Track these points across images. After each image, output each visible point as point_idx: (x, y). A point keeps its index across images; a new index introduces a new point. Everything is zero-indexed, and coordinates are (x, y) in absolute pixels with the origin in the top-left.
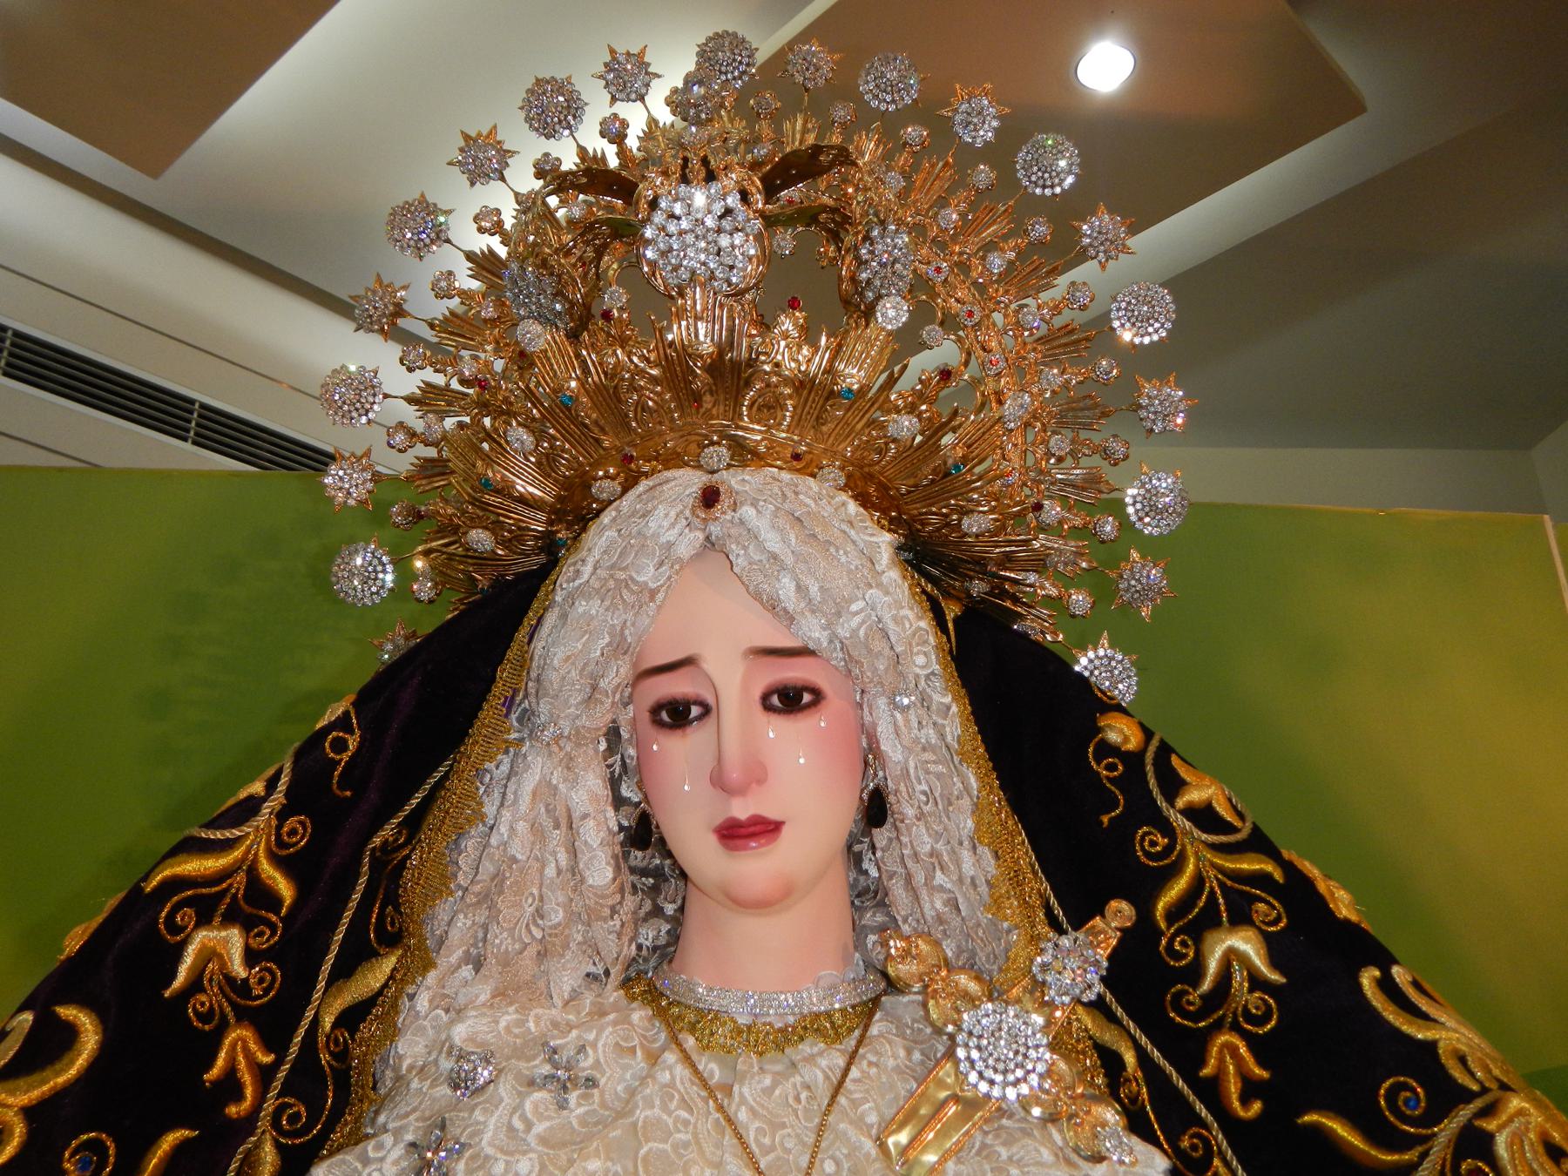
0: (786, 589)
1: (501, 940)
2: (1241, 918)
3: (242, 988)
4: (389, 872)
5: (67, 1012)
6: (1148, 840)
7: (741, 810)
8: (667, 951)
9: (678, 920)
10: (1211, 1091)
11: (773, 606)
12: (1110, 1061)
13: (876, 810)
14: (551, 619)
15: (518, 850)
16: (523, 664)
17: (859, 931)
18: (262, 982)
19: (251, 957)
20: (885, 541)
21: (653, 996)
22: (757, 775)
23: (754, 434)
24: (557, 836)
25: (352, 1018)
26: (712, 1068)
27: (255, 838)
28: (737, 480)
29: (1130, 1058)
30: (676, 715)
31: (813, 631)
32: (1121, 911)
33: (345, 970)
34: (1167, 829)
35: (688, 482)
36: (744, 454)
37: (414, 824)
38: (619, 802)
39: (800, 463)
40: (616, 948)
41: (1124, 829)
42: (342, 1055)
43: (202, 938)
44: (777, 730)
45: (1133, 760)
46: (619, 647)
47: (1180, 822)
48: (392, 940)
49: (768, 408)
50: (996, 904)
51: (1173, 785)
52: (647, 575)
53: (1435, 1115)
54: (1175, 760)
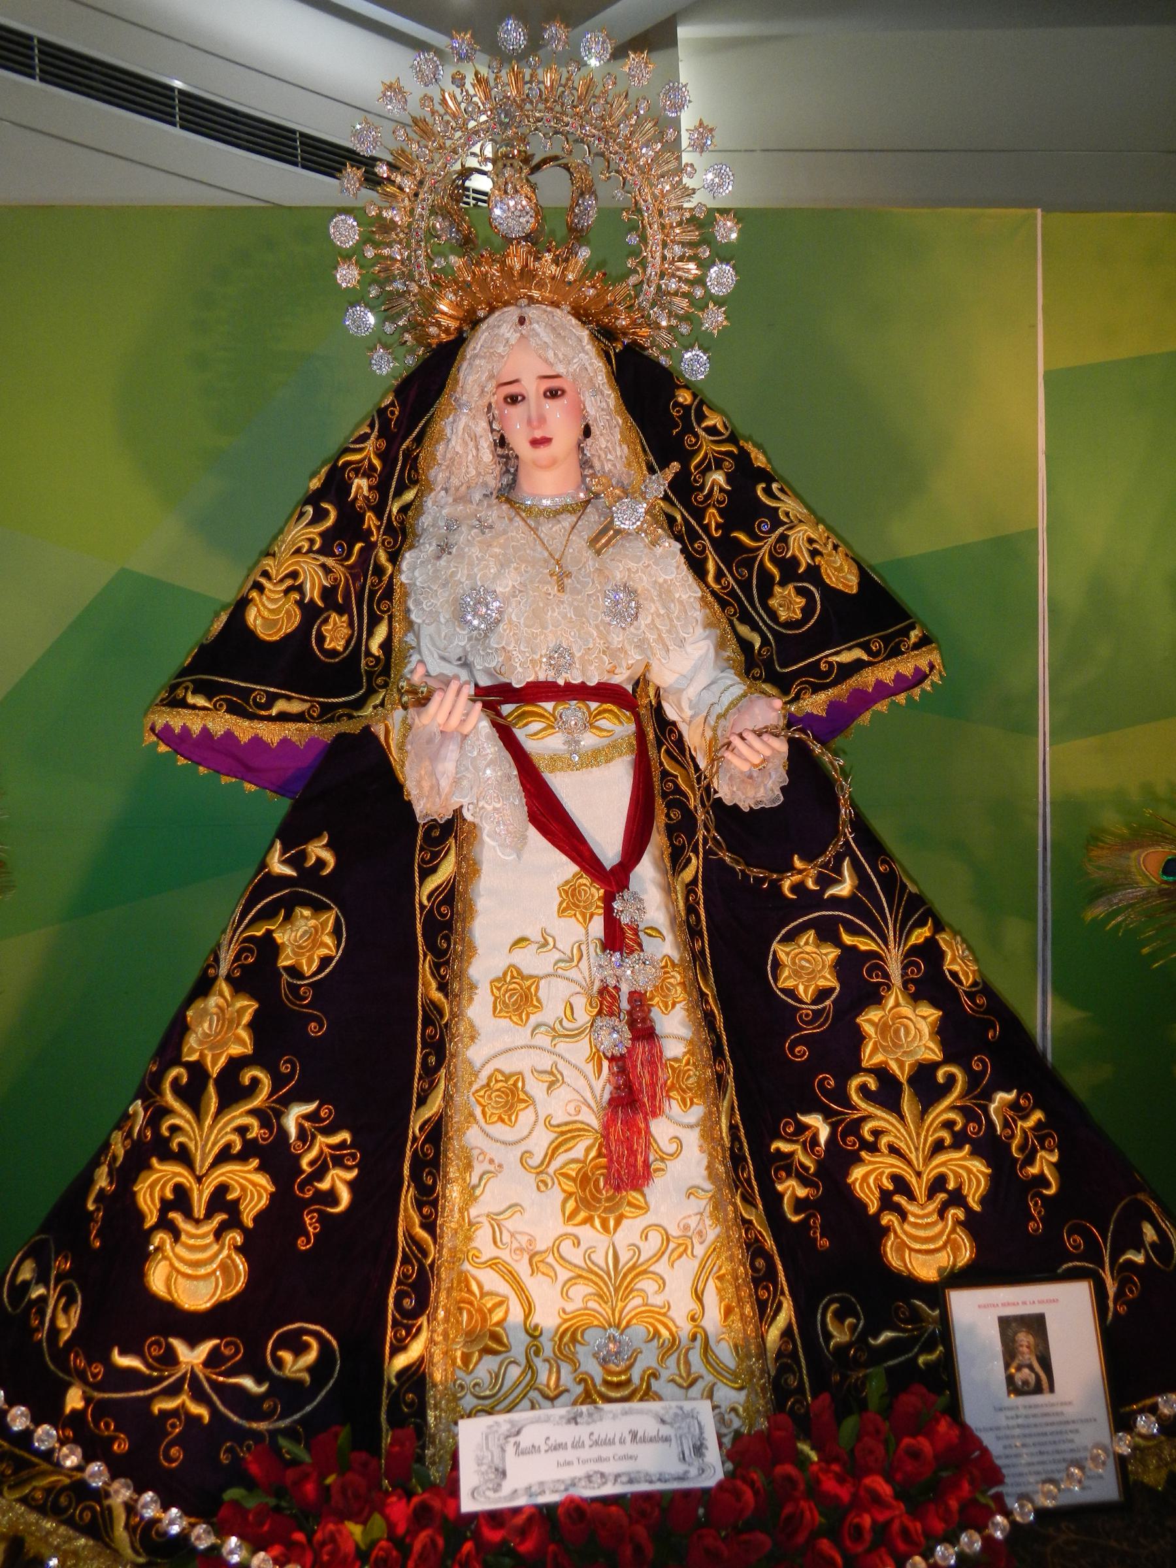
0: (550, 355)
1: (455, 481)
2: (719, 467)
3: (366, 498)
4: (412, 461)
5: (325, 505)
6: (689, 439)
7: (538, 434)
8: (513, 485)
9: (515, 474)
10: (706, 529)
11: (546, 361)
12: (671, 520)
13: (587, 432)
14: (465, 365)
15: (459, 449)
16: (456, 381)
17: (584, 477)
18: (374, 497)
19: (370, 488)
20: (585, 334)
21: (508, 501)
22: (542, 420)
23: (536, 294)
24: (471, 444)
25: (404, 509)
26: (533, 524)
27: (370, 446)
28: (532, 312)
29: (679, 518)
30: (513, 400)
31: (561, 369)
32: (675, 466)
33: (399, 493)
34: (696, 436)
35: (512, 313)
36: (532, 300)
37: (419, 440)
38: (492, 430)
39: (556, 305)
40: (493, 483)
41: (681, 435)
42: (402, 523)
43: (356, 481)
44: (549, 405)
45: (687, 408)
46: (491, 377)
47: (702, 433)
48: (415, 482)
49: (541, 286)
50: (629, 465)
51: (701, 417)
52: (501, 349)
53: (772, 531)
54: (705, 408)
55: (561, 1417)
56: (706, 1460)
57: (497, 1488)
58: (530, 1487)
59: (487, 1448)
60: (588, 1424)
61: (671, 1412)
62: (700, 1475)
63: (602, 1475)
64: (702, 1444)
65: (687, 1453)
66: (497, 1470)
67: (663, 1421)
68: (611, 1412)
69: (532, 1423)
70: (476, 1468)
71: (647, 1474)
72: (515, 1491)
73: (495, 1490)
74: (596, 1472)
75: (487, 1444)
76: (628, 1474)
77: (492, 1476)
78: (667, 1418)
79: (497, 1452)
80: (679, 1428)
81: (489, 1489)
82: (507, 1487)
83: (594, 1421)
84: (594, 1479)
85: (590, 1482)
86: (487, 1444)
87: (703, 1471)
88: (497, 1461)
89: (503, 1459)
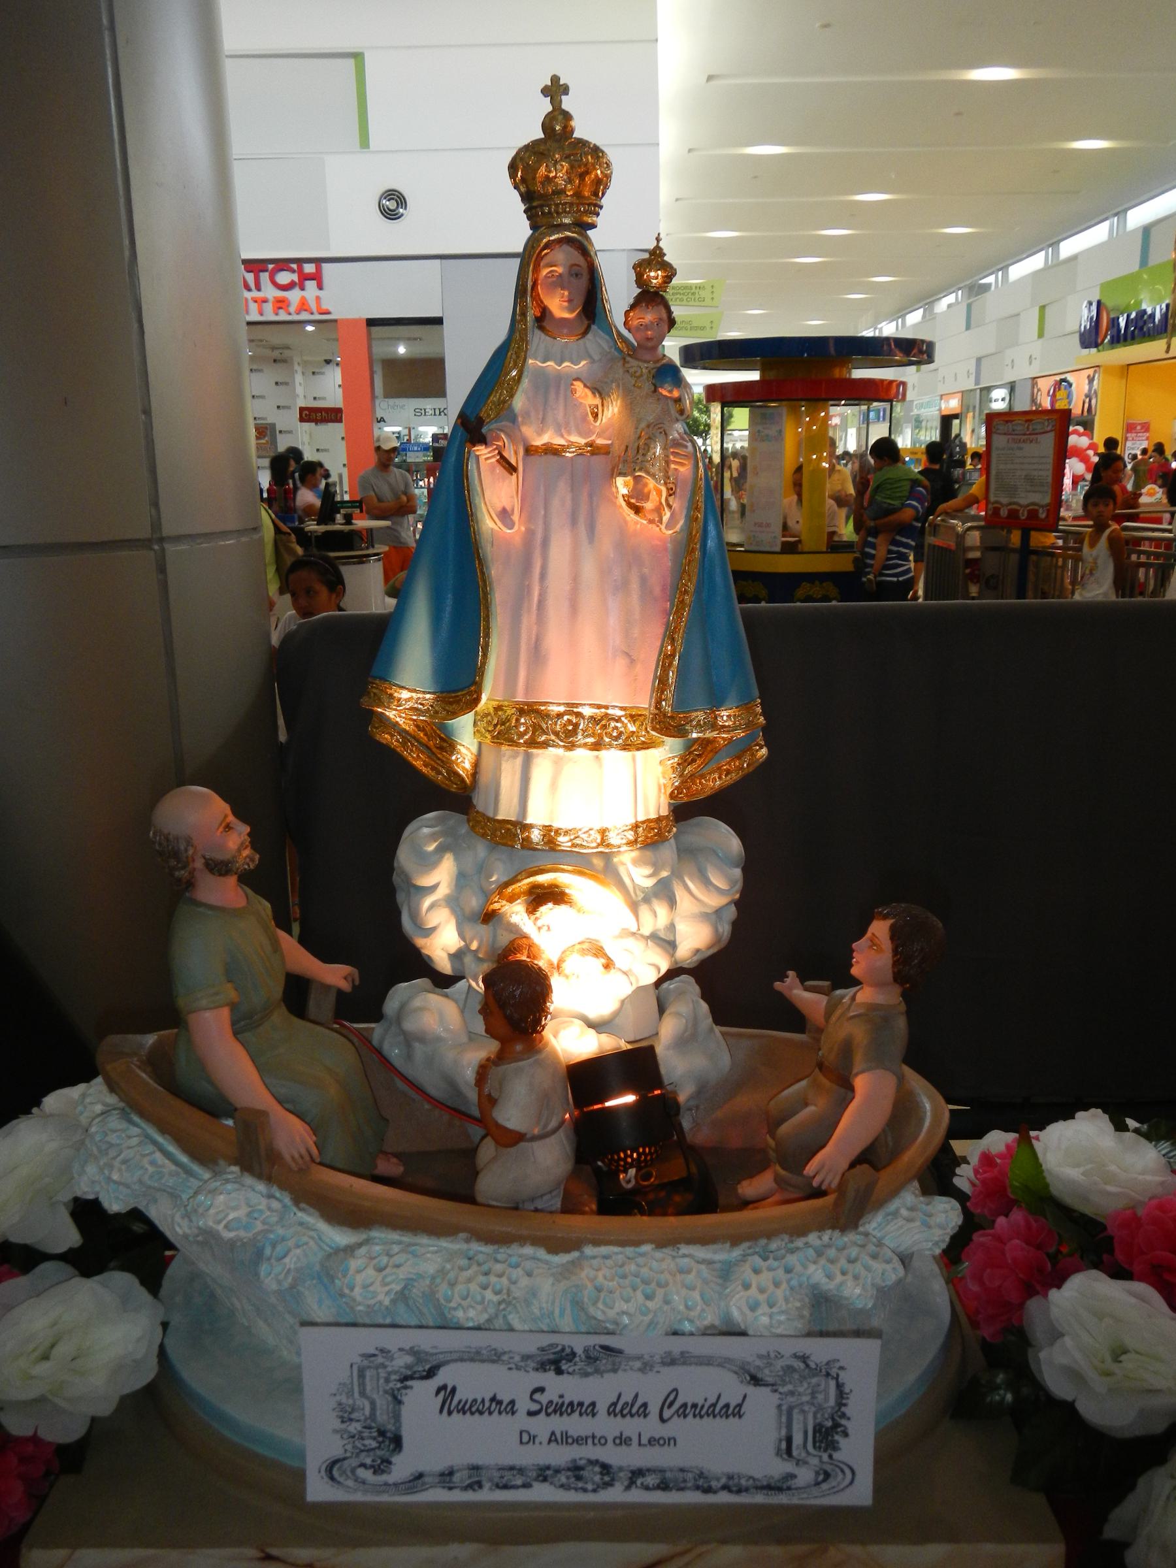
55: (526, 1357)
56: (836, 1455)
57: (382, 1466)
58: (451, 1473)
59: (363, 1393)
60: (586, 1375)
61: (780, 1364)
62: (817, 1484)
63: (605, 1468)
64: (836, 1425)
65: (798, 1439)
66: (382, 1433)
67: (756, 1381)
68: (639, 1358)
69: (462, 1360)
70: (337, 1424)
71: (701, 1475)
72: (420, 1476)
73: (377, 1471)
74: (592, 1463)
75: (362, 1385)
76: (662, 1471)
77: (374, 1444)
78: (767, 1375)
79: (383, 1402)
80: (792, 1393)
81: (363, 1465)
82: (402, 1467)
83: (597, 1371)
84: (584, 1473)
85: (579, 1478)
86: (362, 1385)
87: (827, 1476)
88: (382, 1418)
89: (397, 1417)
